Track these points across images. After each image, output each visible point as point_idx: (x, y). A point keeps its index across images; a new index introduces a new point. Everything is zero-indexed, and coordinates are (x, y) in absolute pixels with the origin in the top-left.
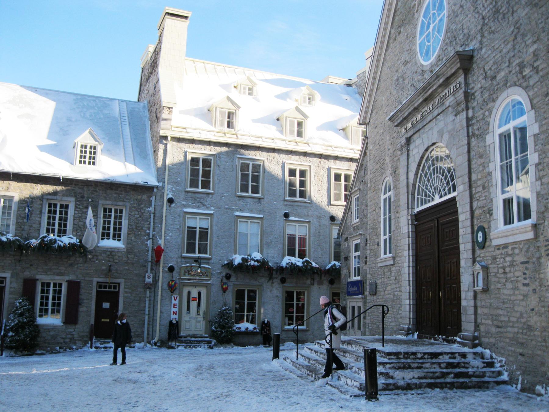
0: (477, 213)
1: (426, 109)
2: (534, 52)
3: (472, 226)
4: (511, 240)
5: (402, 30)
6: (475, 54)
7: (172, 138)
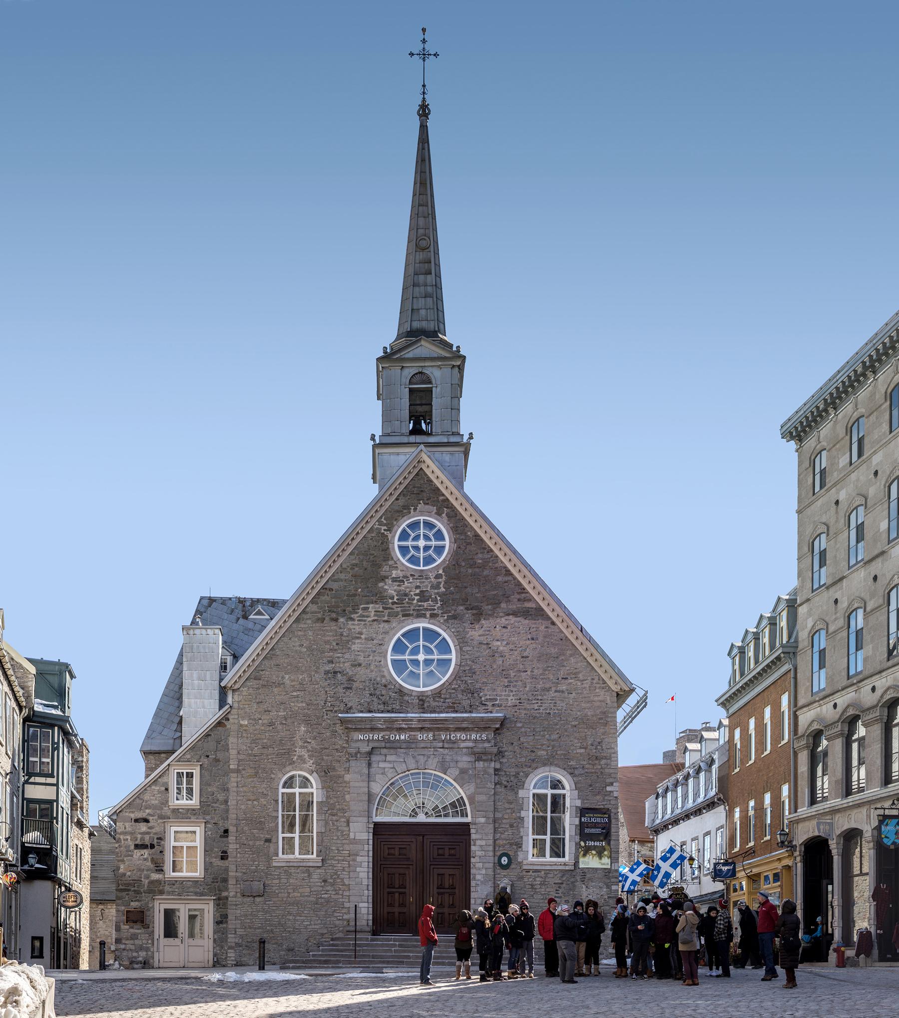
0: (500, 842)
1: (420, 736)
3: (494, 851)
4: (548, 868)
5: (342, 620)
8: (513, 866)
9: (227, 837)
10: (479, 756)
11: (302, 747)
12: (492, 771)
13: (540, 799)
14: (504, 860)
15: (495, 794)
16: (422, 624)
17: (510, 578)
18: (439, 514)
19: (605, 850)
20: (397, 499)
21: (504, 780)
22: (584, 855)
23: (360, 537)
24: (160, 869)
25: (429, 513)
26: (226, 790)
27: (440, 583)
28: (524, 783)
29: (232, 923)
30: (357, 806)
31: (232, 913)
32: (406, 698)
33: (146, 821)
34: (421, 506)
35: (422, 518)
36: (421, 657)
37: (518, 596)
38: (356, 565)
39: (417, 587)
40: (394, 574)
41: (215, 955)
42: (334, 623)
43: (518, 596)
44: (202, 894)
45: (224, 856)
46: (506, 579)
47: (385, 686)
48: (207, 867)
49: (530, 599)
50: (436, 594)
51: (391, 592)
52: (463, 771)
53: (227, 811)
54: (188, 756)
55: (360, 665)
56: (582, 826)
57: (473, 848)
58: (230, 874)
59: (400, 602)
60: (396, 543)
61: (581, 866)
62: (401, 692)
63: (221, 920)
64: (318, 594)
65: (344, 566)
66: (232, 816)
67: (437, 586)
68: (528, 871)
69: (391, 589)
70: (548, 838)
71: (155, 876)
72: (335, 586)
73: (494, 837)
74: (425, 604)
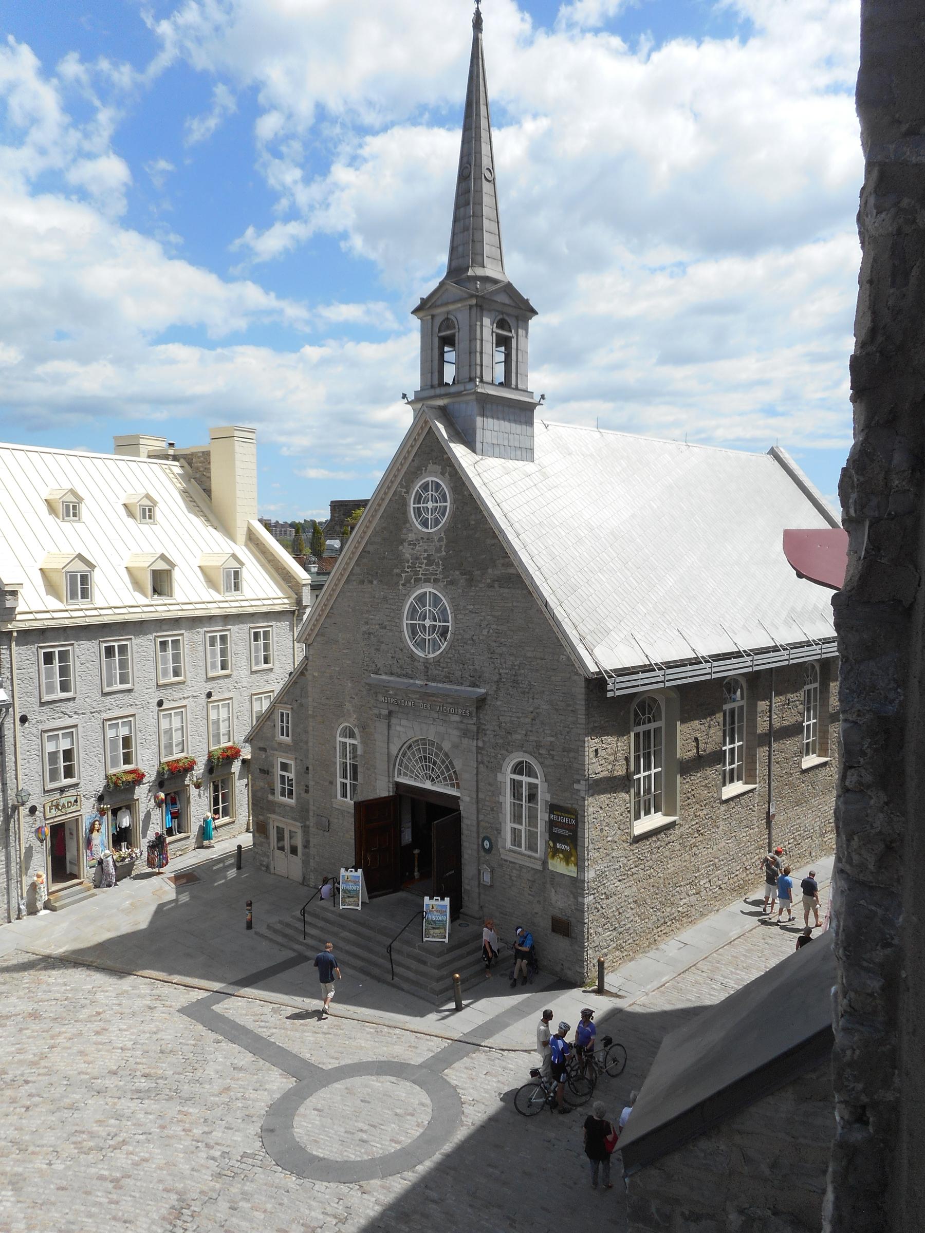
0: (482, 823)
2: (551, 742)
3: (478, 832)
5: (375, 582)
6: (489, 698)
7: (17, 631)
8: (493, 852)
9: (308, 773)
10: (465, 734)
11: (350, 702)
12: (474, 749)
13: (516, 785)
14: (486, 843)
15: (477, 774)
16: (428, 589)
17: (496, 541)
18: (443, 474)
19: (572, 855)
20: (413, 461)
21: (486, 759)
22: (553, 857)
23: (387, 501)
24: (273, 792)
25: (434, 473)
26: (306, 732)
27: (441, 546)
28: (502, 766)
29: (312, 851)
30: (381, 764)
31: (313, 841)
32: (416, 663)
33: (263, 749)
34: (430, 467)
35: (430, 479)
36: (428, 623)
37: (502, 561)
38: (385, 528)
39: (426, 551)
40: (411, 537)
41: (304, 874)
42: (370, 586)
43: (502, 561)
44: (295, 820)
45: (307, 791)
46: (493, 542)
47: (401, 650)
48: (298, 795)
49: (513, 565)
50: (439, 557)
51: (408, 556)
52: (455, 746)
53: (308, 750)
54: (285, 699)
55: (385, 628)
56: (551, 824)
57: (463, 826)
58: (311, 807)
59: (412, 567)
60: (412, 505)
61: (550, 867)
62: (412, 657)
63: (306, 846)
64: (361, 556)
65: (377, 529)
66: (311, 756)
67: (438, 550)
68: (506, 861)
69: (407, 552)
70: (523, 828)
71: (270, 797)
72: (370, 548)
73: (478, 818)
74: (431, 568)
